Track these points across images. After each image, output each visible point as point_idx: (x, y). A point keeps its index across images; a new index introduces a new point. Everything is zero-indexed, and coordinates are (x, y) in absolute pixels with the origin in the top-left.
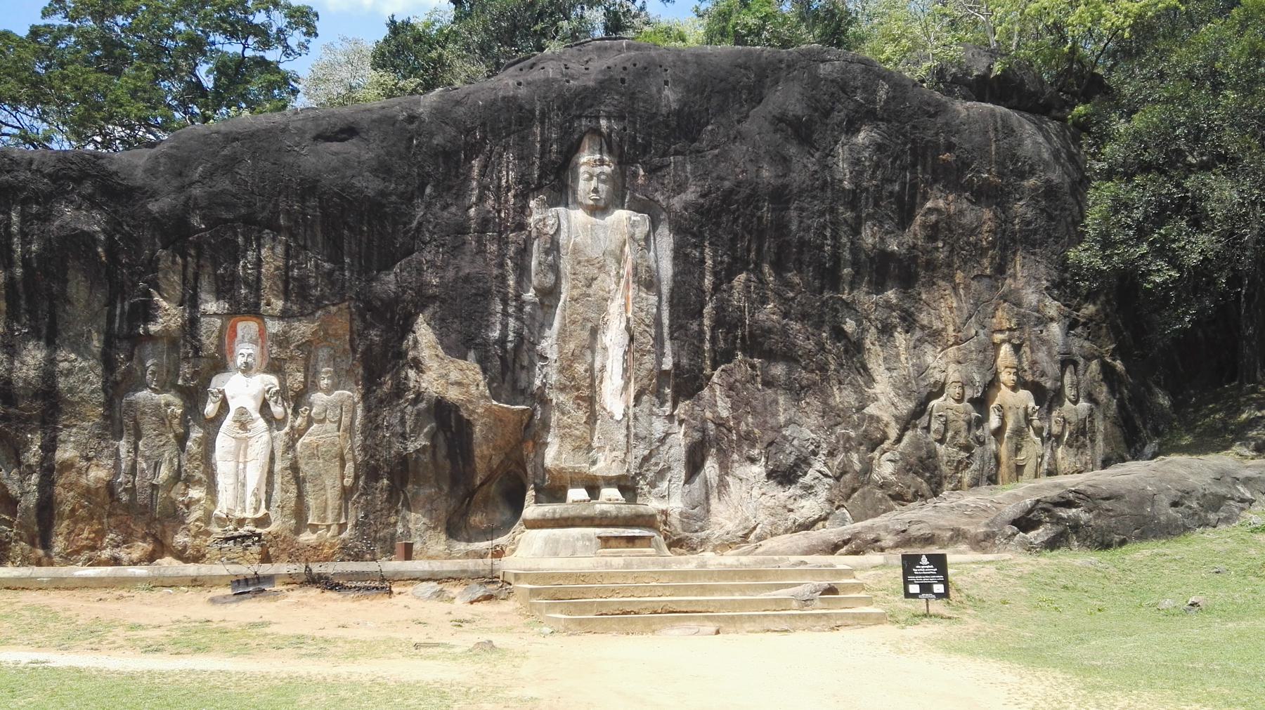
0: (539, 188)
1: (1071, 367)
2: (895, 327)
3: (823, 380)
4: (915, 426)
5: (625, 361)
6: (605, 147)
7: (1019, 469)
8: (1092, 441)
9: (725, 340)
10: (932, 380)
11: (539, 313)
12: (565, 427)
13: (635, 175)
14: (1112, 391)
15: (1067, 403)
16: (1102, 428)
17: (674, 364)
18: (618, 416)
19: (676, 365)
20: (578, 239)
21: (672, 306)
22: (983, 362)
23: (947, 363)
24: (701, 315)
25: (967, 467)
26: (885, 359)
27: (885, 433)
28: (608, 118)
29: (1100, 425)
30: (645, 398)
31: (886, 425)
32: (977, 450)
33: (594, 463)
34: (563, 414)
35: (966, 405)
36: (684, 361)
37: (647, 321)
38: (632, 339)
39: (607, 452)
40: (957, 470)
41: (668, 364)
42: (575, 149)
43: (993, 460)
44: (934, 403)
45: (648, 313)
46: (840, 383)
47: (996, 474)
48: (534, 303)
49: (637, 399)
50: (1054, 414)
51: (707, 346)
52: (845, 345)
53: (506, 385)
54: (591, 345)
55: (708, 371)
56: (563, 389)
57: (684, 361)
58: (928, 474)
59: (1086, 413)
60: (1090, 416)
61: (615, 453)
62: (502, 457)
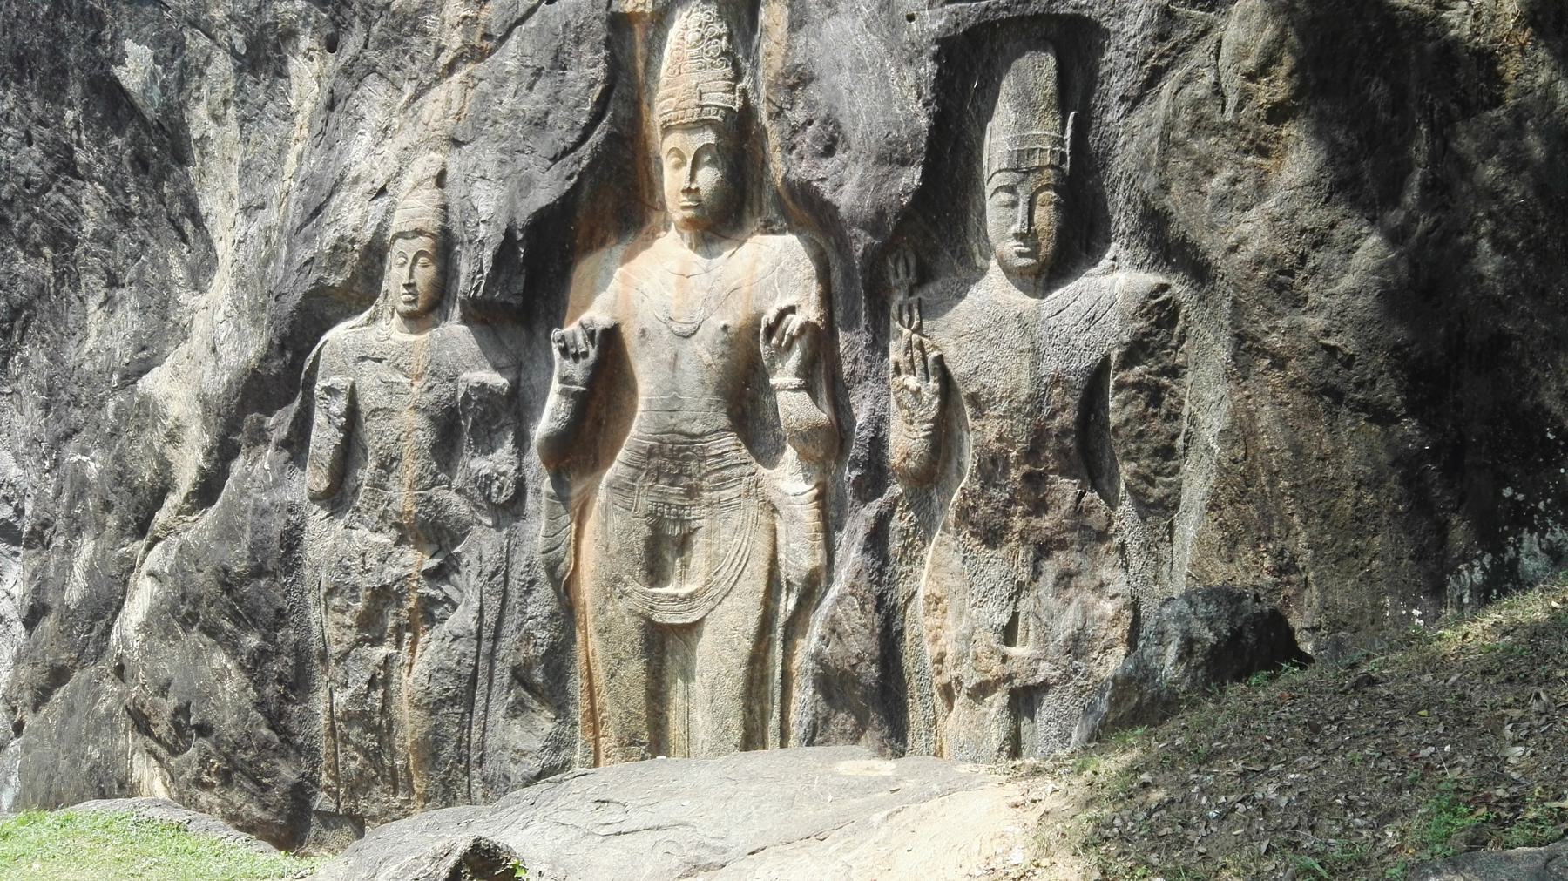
1: (1036, 71)
2: (290, 34)
3: (60, 279)
4: (259, 437)
7: (664, 645)
8: (1159, 510)
10: (330, 236)
14: (1358, 180)
15: (993, 293)
16: (1211, 426)
22: (539, 124)
23: (407, 155)
25: (428, 613)
26: (246, 168)
27: (165, 465)
29: (1208, 400)
31: (173, 438)
32: (482, 545)
35: (455, 332)
40: (370, 627)
43: (544, 592)
44: (339, 335)
46: (113, 282)
47: (558, 658)
50: (896, 354)
52: (135, 141)
58: (252, 641)
59: (1114, 333)
60: (1135, 352)
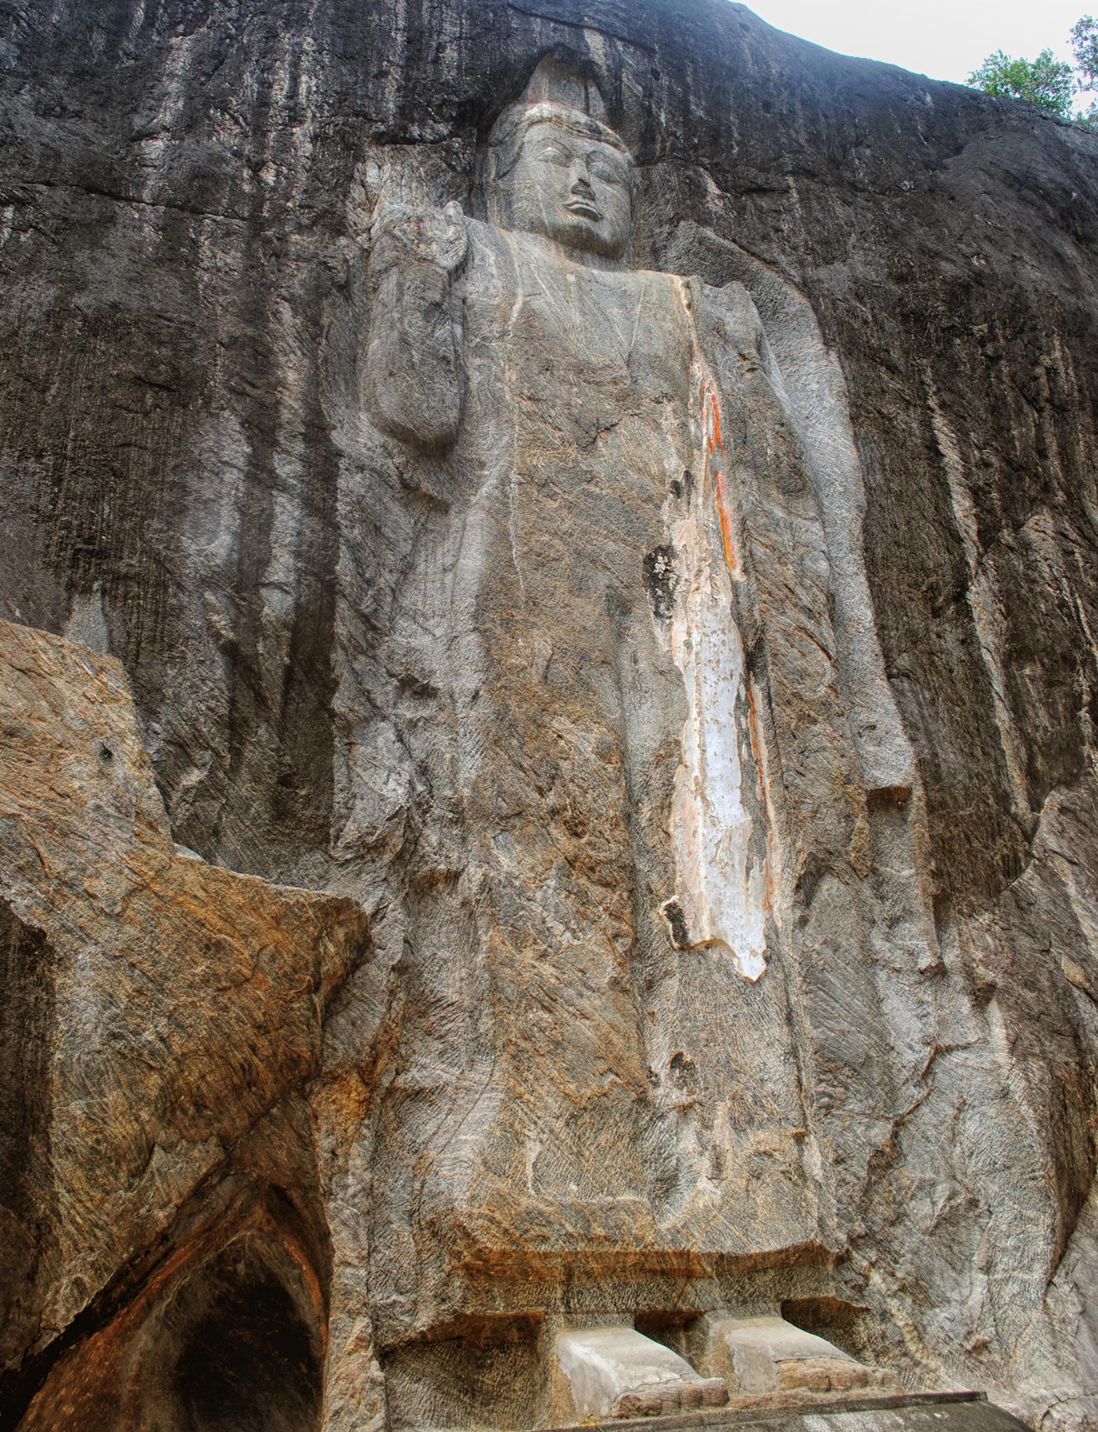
0: (396, 139)
5: (745, 737)
6: (599, 107)
9: (1050, 706)
11: (399, 519)
12: (527, 999)
13: (697, 191)
17: (921, 764)
18: (752, 967)
19: (929, 768)
20: (537, 304)
21: (872, 565)
24: (965, 612)
28: (608, 34)
30: (829, 887)
33: (667, 1184)
34: (518, 938)
36: (950, 757)
37: (806, 600)
38: (753, 661)
39: (722, 1133)
41: (894, 763)
42: (508, 85)
45: (802, 575)
48: (381, 475)
49: (806, 887)
51: (1002, 717)
53: (243, 788)
54: (603, 661)
55: (1021, 805)
56: (512, 818)
57: (950, 757)
61: (764, 1137)
62: (203, 1157)
